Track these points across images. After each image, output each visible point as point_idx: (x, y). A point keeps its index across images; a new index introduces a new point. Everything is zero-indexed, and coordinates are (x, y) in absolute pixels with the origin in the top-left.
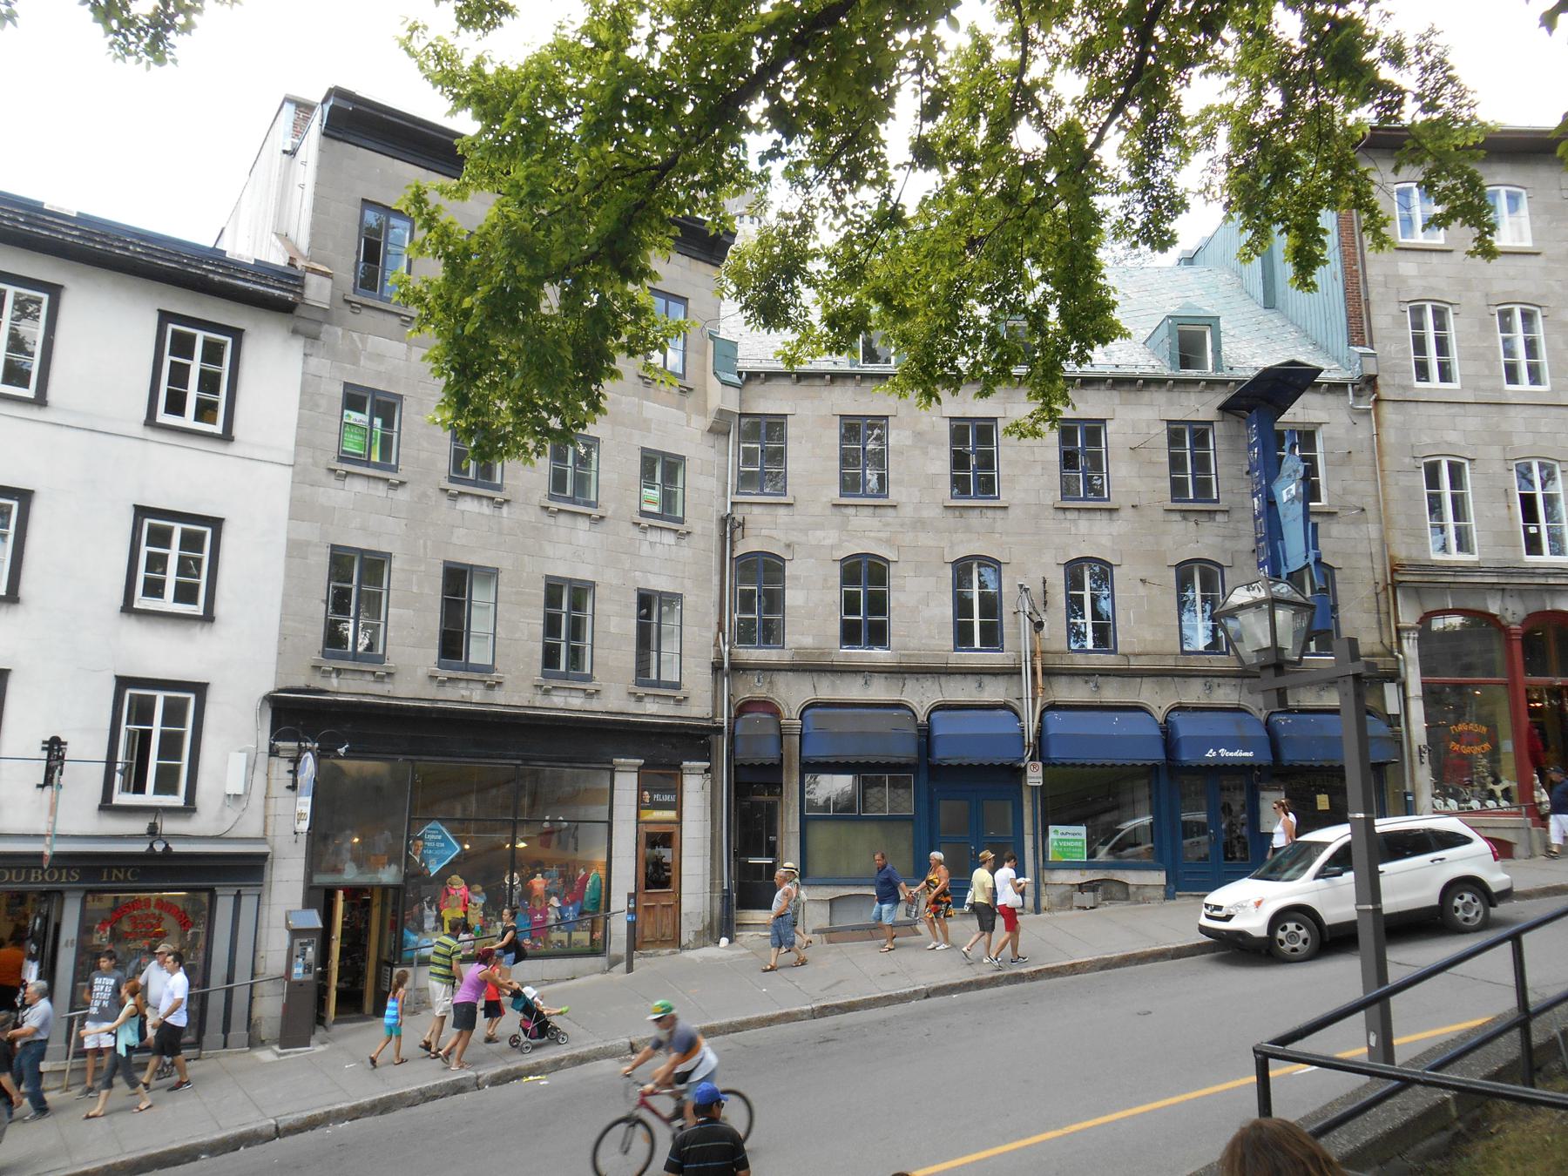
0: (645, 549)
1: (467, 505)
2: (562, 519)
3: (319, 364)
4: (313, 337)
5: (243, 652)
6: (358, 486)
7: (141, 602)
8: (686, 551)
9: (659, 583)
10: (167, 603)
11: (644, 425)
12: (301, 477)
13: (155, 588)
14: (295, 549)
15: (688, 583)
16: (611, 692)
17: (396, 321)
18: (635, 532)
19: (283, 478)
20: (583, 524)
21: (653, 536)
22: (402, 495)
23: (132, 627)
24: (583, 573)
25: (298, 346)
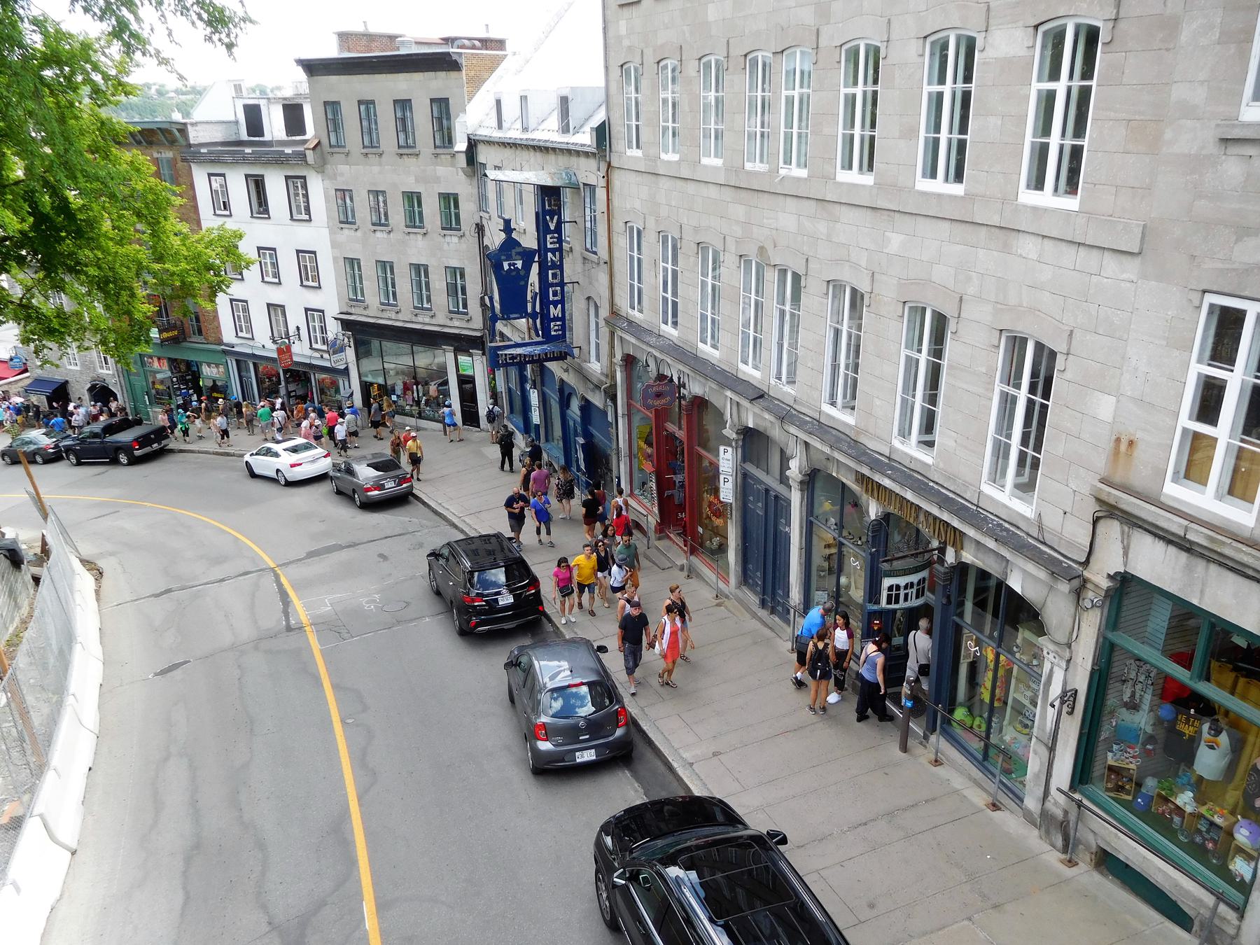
3: (327, 182)
5: (330, 300)
6: (346, 232)
7: (305, 283)
9: (455, 263)
10: (310, 283)
11: (437, 180)
12: (332, 233)
13: (307, 279)
14: (335, 259)
18: (442, 239)
21: (448, 239)
22: (359, 233)
23: (303, 289)
25: (319, 176)
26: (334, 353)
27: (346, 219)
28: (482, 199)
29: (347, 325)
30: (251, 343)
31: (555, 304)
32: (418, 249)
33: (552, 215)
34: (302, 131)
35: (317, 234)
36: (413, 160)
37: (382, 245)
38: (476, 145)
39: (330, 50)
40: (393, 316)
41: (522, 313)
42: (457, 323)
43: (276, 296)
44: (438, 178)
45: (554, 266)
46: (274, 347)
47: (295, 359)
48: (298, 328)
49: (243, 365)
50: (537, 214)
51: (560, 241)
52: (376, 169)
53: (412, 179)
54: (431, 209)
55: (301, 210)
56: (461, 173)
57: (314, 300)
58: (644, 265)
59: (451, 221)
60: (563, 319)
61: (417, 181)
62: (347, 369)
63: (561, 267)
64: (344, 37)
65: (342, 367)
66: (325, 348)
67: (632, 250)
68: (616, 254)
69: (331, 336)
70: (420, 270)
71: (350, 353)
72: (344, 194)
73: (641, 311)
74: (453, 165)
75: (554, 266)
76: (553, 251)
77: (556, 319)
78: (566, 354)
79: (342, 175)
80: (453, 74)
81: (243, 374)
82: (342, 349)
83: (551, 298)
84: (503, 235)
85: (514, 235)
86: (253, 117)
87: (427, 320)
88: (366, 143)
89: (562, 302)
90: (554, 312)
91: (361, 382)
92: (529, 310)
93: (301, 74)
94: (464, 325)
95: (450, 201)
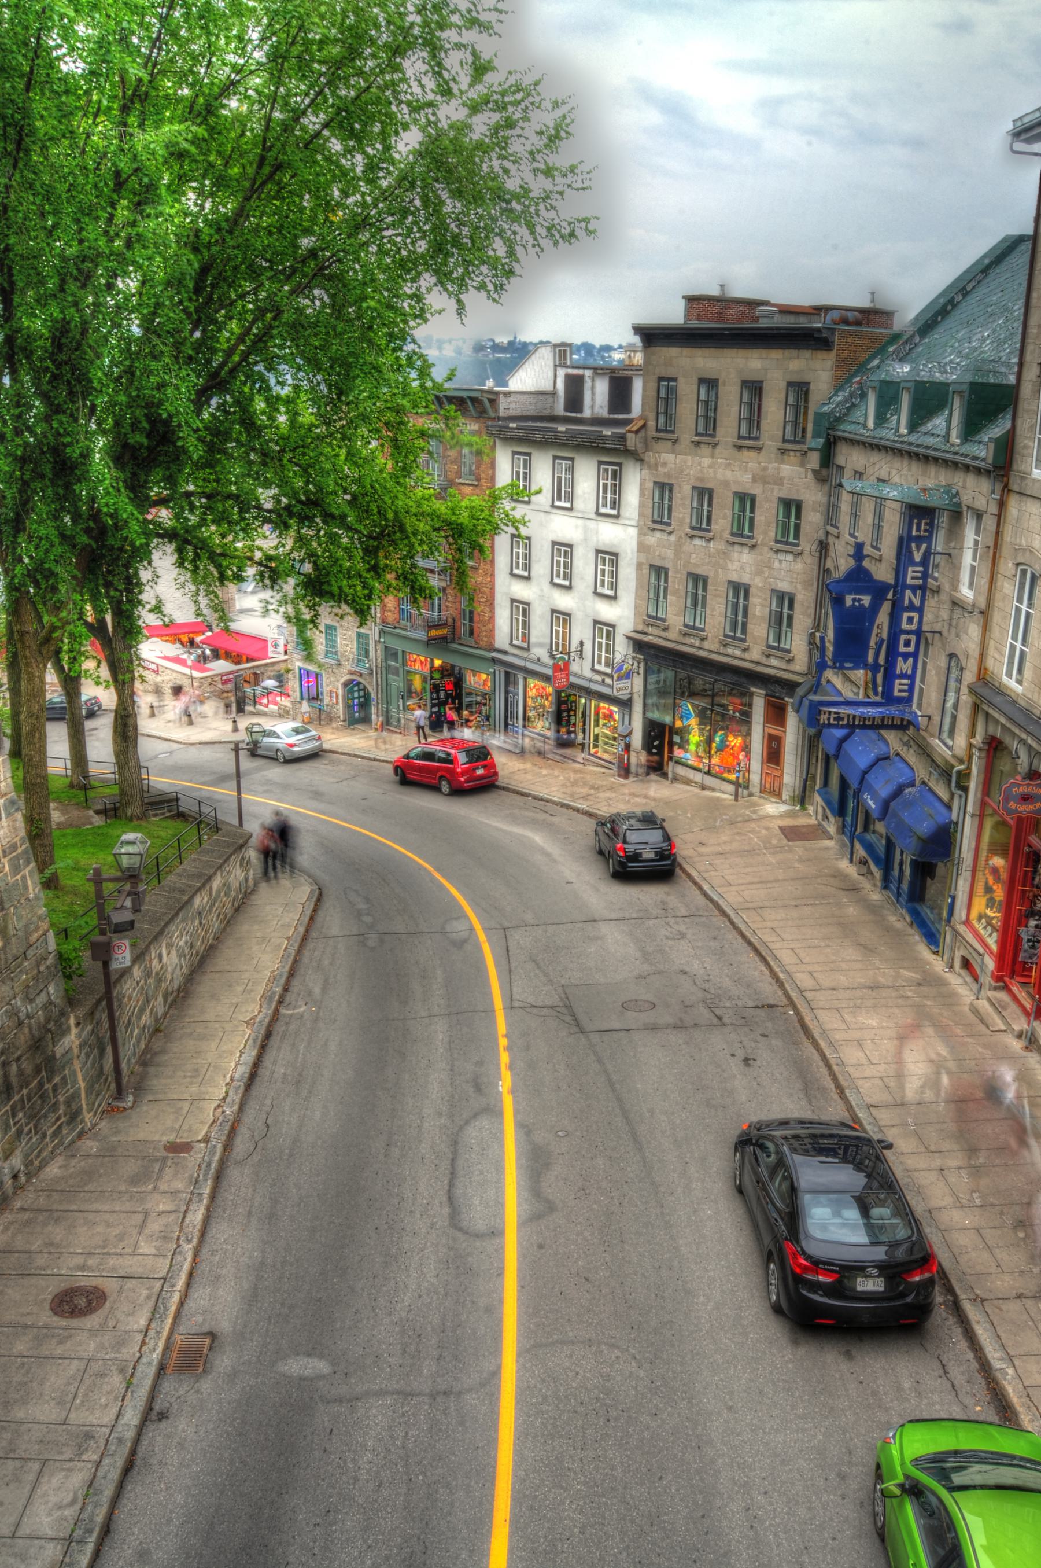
0: (776, 564)
1: (697, 542)
2: (737, 547)
4: (642, 461)
5: (622, 614)
6: (658, 534)
8: (799, 566)
9: (784, 586)
11: (779, 481)
12: (641, 534)
13: (603, 585)
14: (639, 566)
15: (799, 586)
16: (753, 653)
17: (670, 443)
18: (771, 554)
19: (633, 532)
20: (746, 550)
21: (781, 556)
22: (673, 538)
24: (746, 579)
25: (638, 466)
26: (619, 679)
27: (659, 517)
28: (831, 513)
29: (639, 646)
30: (525, 654)
31: (906, 656)
32: (741, 564)
33: (919, 540)
34: (627, 409)
35: (622, 535)
36: (752, 454)
37: (698, 554)
38: (835, 443)
39: (674, 314)
40: (697, 643)
41: (859, 661)
42: (774, 662)
43: (564, 601)
44: (782, 479)
45: (911, 607)
46: (551, 662)
47: (572, 679)
48: (582, 644)
49: (512, 679)
50: (901, 539)
51: (925, 576)
52: (706, 461)
53: (747, 478)
54: (766, 515)
55: (611, 506)
56: (810, 475)
57: (607, 612)
58: (1033, 623)
59: (789, 534)
60: (912, 677)
61: (754, 480)
62: (630, 700)
63: (920, 610)
64: (692, 301)
65: (626, 697)
66: (609, 671)
67: (1020, 600)
68: (998, 603)
69: (618, 658)
70: (740, 590)
71: (638, 682)
72: (664, 488)
73: (1019, 682)
74: (802, 464)
75: (911, 607)
76: (914, 589)
78: (909, 723)
79: (665, 464)
80: (821, 355)
81: (511, 689)
82: (628, 675)
83: (902, 649)
84: (852, 562)
85: (866, 563)
86: (575, 385)
87: (738, 653)
88: (701, 430)
89: (915, 655)
90: (903, 666)
91: (644, 718)
92: (870, 659)
93: (636, 340)
94: (784, 666)
95: (792, 507)
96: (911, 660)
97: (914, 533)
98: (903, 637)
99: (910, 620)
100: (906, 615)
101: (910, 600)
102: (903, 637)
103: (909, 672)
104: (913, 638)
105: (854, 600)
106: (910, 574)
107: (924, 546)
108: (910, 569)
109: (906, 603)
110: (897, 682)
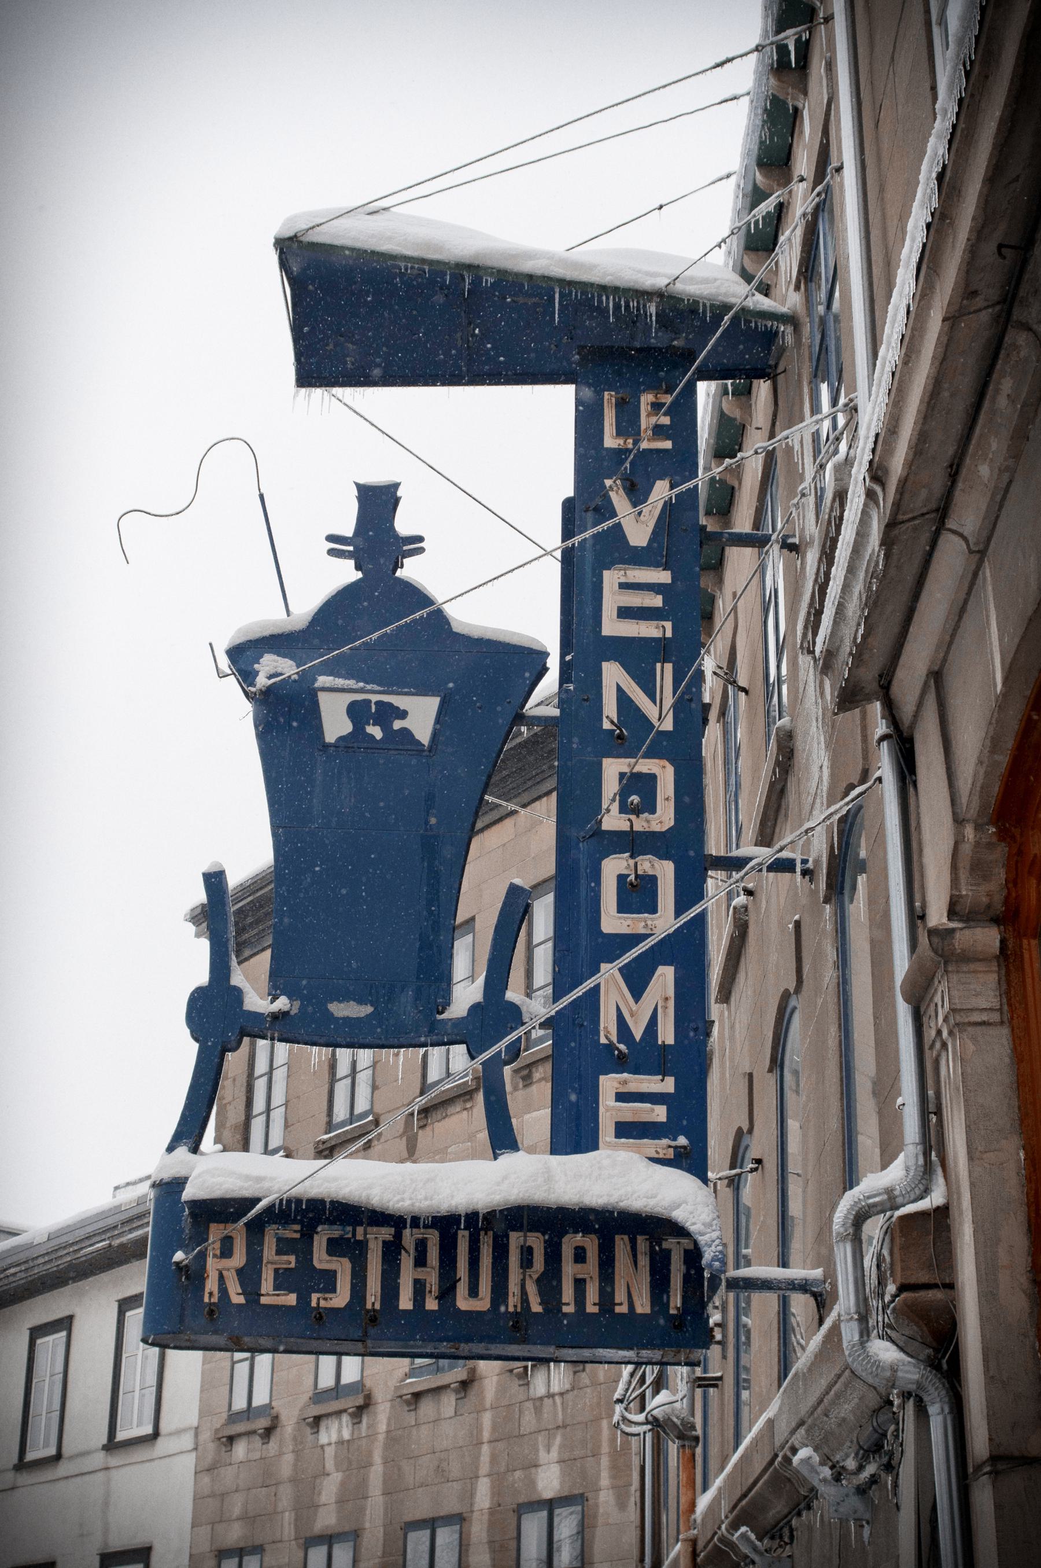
45: (632, 734)
63: (683, 748)
75: (632, 734)
76: (638, 657)
77: (641, 1055)
83: (613, 921)
96: (665, 977)
97: (611, 441)
98: (614, 867)
99: (639, 790)
100: (613, 769)
101: (623, 698)
102: (614, 867)
103: (667, 1035)
104: (665, 872)
105: (356, 711)
106: (611, 600)
107: (661, 491)
108: (611, 578)
109: (610, 708)
110: (609, 1084)
